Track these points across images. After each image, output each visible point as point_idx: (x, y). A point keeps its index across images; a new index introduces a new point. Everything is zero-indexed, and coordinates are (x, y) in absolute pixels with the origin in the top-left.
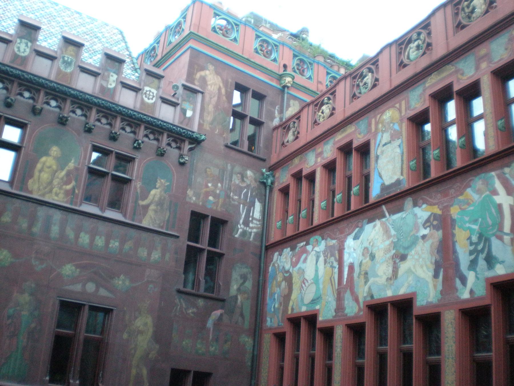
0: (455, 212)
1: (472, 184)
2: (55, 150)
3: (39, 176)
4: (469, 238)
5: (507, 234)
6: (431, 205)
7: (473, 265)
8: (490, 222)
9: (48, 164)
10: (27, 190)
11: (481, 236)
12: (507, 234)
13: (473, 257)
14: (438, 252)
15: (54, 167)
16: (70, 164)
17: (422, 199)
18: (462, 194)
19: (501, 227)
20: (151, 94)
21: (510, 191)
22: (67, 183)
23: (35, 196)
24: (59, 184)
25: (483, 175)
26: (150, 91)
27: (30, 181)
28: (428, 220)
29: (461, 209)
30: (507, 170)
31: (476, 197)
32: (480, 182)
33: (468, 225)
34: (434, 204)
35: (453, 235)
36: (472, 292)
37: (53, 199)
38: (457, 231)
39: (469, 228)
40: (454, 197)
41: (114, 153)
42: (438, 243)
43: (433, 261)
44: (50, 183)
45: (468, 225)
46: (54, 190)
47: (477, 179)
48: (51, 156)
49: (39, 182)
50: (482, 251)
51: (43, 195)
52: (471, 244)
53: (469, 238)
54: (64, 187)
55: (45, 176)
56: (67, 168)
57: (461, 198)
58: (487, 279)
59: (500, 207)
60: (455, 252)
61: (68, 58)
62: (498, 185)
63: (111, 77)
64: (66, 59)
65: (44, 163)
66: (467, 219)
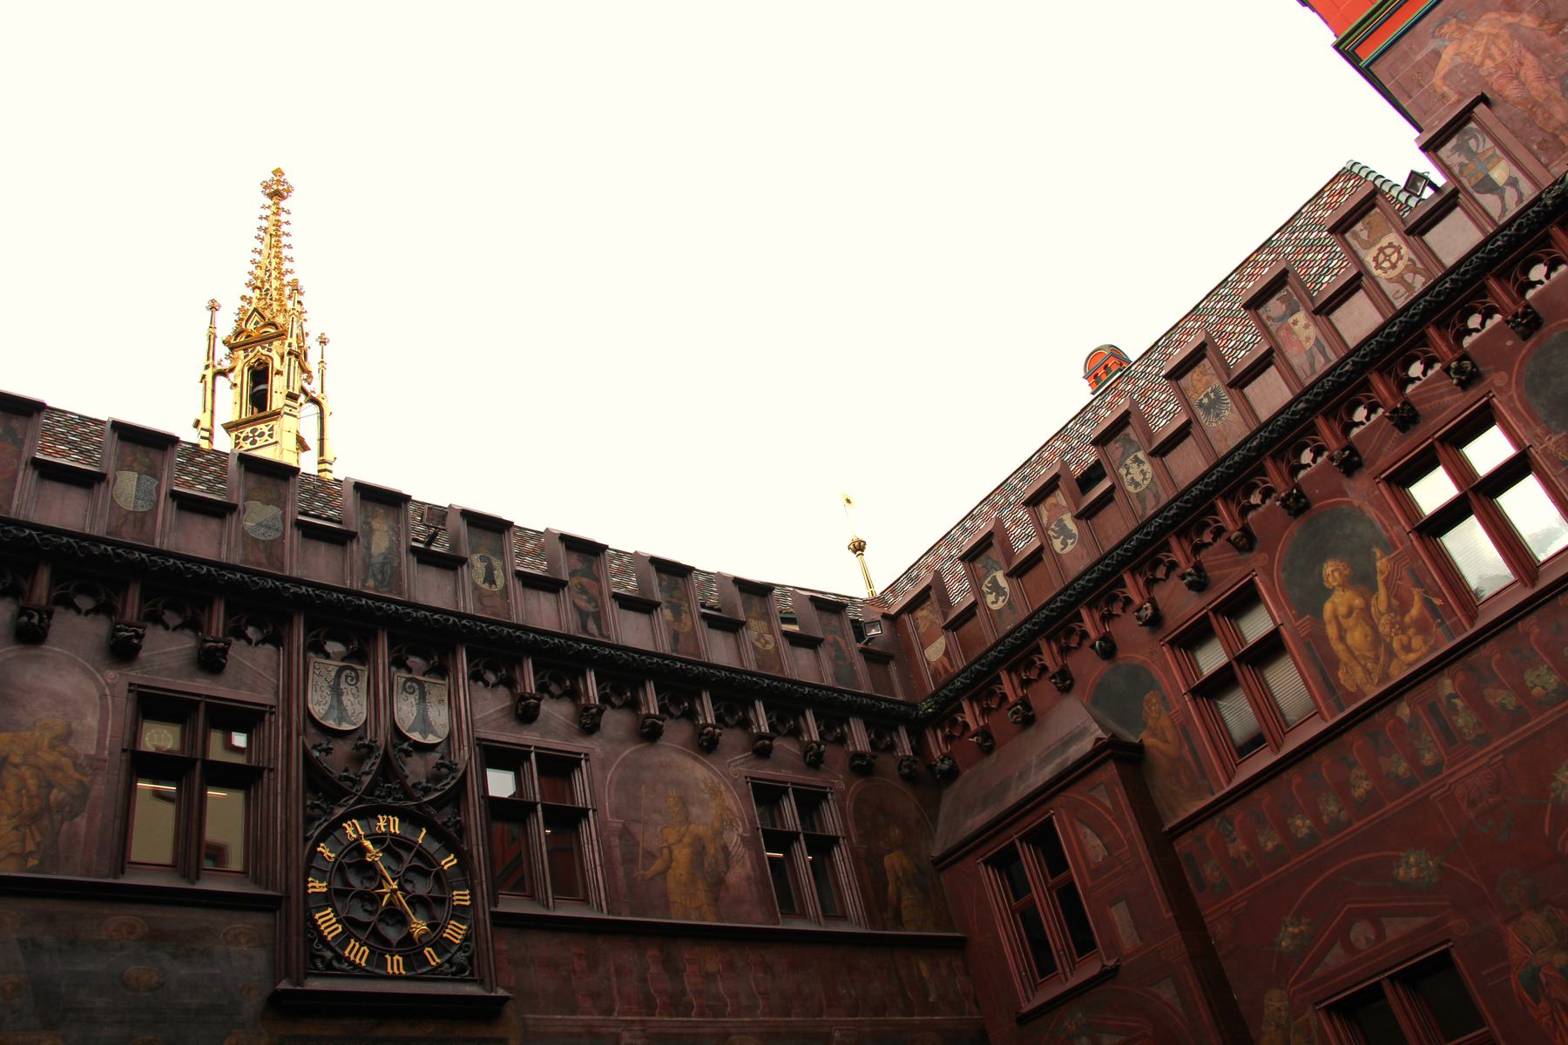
2: (1331, 571)
3: (1349, 649)
9: (1342, 610)
10: (1353, 697)
15: (1358, 602)
16: (1378, 564)
20: (1389, 251)
22: (1404, 608)
23: (1373, 692)
24: (1392, 625)
26: (1381, 250)
27: (1340, 674)
37: (1410, 665)
41: (1437, 445)
44: (1377, 639)
46: (1395, 645)
48: (1334, 589)
49: (1355, 658)
51: (1385, 676)
54: (1407, 619)
55: (1356, 637)
56: (1380, 578)
61: (1207, 395)
63: (1296, 328)
64: (1206, 401)
65: (1336, 617)
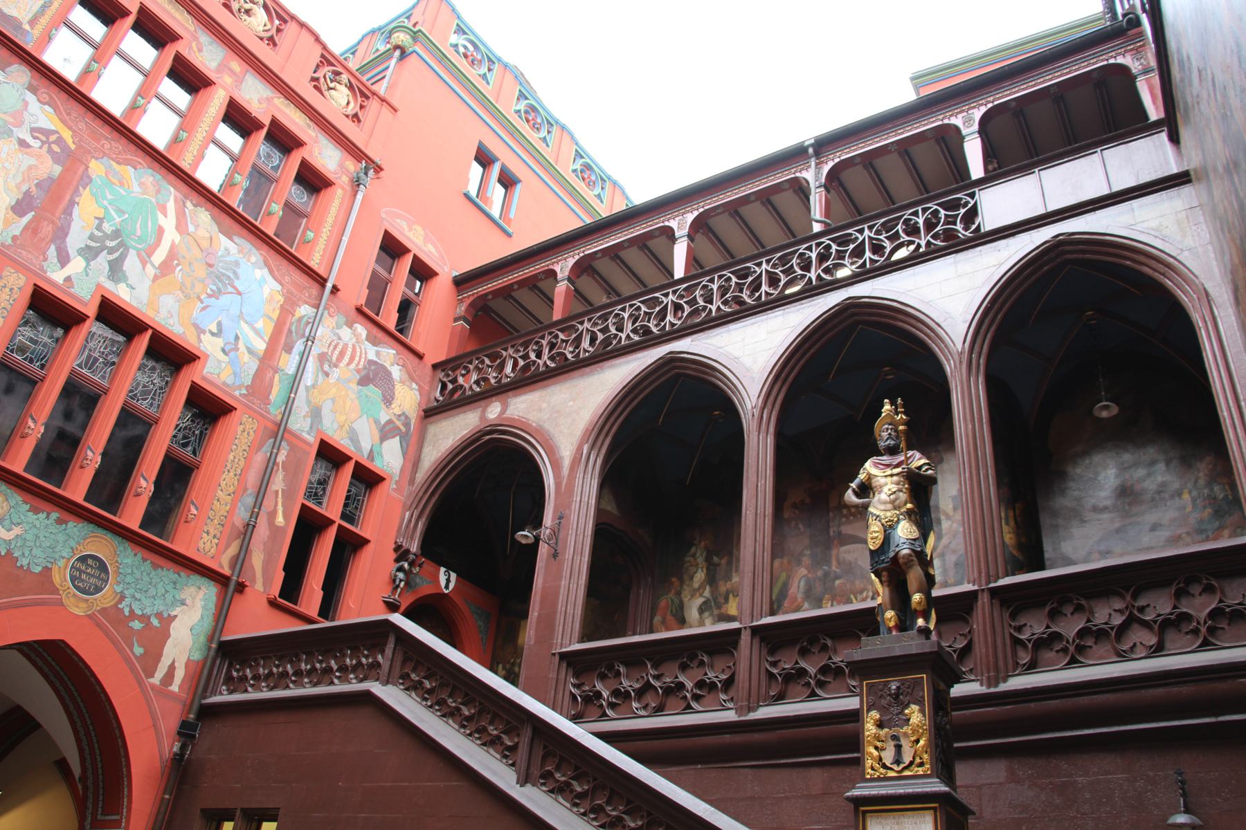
0: (96, 168)
1: (140, 171)
4: (101, 220)
5: (153, 265)
6: (63, 121)
7: (89, 253)
8: (139, 233)
11: (117, 234)
12: (153, 265)
13: (93, 244)
14: (38, 185)
17: (51, 97)
18: (118, 163)
19: (150, 251)
21: (181, 226)
25: (159, 177)
28: (47, 133)
29: (106, 173)
30: (189, 204)
31: (136, 188)
32: (151, 179)
33: (106, 203)
34: (70, 128)
35: (76, 191)
36: (68, 279)
38: (86, 193)
39: (106, 208)
40: (105, 154)
42: (45, 176)
43: (24, 188)
45: (106, 203)
47: (150, 171)
50: (111, 251)
52: (99, 228)
53: (101, 220)
57: (114, 164)
58: (99, 286)
59: (161, 231)
60: (68, 212)
62: (171, 206)
66: (110, 197)
